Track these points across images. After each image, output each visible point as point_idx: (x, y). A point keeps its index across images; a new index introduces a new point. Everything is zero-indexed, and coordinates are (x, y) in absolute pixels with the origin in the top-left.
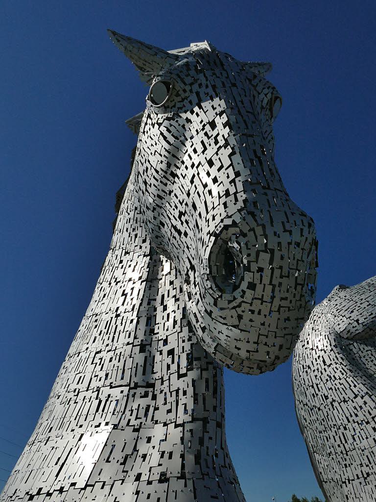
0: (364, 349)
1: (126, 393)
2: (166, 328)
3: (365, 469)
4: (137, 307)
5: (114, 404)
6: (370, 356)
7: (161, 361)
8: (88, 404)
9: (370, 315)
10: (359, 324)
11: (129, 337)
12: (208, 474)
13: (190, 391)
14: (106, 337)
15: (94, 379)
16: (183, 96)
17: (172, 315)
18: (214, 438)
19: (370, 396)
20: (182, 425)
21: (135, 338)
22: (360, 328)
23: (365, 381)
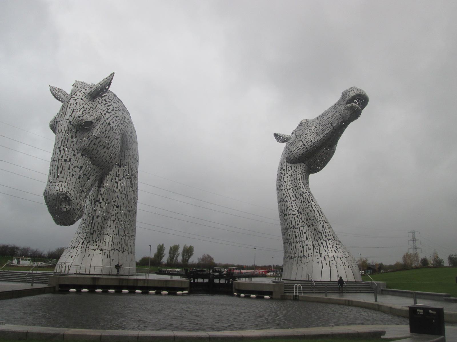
0: (295, 170)
6: (295, 175)
9: (297, 148)
10: (291, 154)
12: (83, 247)
18: (89, 238)
19: (284, 201)
22: (292, 157)
23: (285, 192)
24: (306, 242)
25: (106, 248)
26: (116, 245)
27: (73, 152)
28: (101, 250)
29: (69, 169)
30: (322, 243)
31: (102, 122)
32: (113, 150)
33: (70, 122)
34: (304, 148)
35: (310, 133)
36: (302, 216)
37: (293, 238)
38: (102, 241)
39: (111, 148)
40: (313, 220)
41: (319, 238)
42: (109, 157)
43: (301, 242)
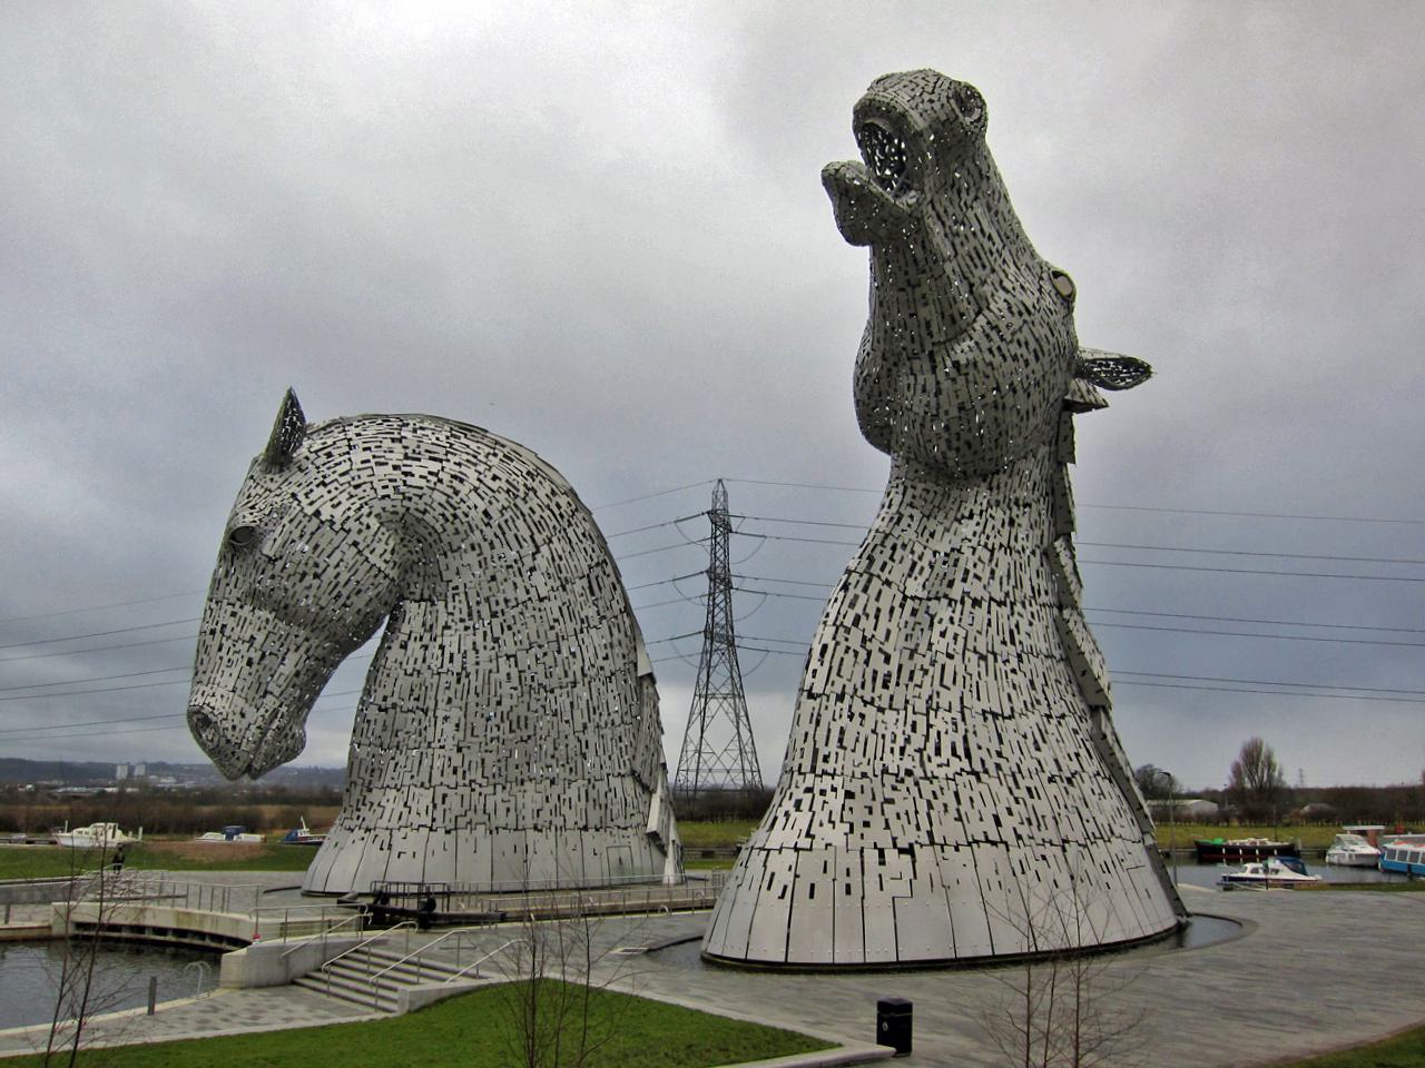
25: (383, 823)
26: (418, 814)
27: (230, 608)
28: (368, 830)
29: (220, 649)
31: (292, 517)
32: (338, 574)
38: (375, 807)
39: (331, 572)
42: (330, 594)
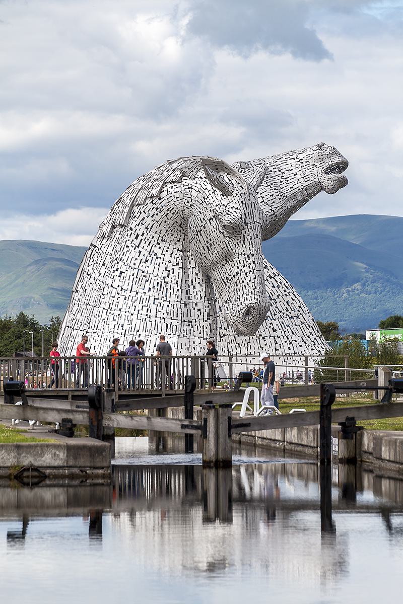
1: (180, 323)
2: (196, 298)
3: (223, 331)
4: (179, 283)
5: (175, 327)
7: (194, 314)
8: (160, 325)
11: (178, 298)
13: (209, 327)
14: (161, 292)
15: (159, 313)
16: (238, 233)
17: (199, 293)
20: (206, 339)
21: (181, 299)
24: (294, 337)
30: (315, 339)
33: (261, 226)
34: (272, 215)
35: (278, 195)
36: (278, 304)
37: (266, 330)
40: (299, 311)
41: (311, 333)
43: (285, 337)
